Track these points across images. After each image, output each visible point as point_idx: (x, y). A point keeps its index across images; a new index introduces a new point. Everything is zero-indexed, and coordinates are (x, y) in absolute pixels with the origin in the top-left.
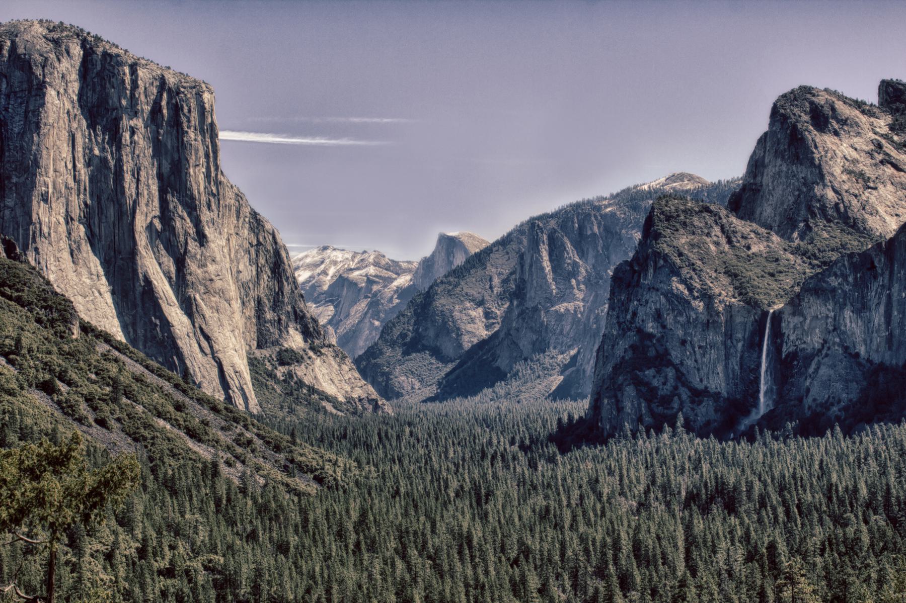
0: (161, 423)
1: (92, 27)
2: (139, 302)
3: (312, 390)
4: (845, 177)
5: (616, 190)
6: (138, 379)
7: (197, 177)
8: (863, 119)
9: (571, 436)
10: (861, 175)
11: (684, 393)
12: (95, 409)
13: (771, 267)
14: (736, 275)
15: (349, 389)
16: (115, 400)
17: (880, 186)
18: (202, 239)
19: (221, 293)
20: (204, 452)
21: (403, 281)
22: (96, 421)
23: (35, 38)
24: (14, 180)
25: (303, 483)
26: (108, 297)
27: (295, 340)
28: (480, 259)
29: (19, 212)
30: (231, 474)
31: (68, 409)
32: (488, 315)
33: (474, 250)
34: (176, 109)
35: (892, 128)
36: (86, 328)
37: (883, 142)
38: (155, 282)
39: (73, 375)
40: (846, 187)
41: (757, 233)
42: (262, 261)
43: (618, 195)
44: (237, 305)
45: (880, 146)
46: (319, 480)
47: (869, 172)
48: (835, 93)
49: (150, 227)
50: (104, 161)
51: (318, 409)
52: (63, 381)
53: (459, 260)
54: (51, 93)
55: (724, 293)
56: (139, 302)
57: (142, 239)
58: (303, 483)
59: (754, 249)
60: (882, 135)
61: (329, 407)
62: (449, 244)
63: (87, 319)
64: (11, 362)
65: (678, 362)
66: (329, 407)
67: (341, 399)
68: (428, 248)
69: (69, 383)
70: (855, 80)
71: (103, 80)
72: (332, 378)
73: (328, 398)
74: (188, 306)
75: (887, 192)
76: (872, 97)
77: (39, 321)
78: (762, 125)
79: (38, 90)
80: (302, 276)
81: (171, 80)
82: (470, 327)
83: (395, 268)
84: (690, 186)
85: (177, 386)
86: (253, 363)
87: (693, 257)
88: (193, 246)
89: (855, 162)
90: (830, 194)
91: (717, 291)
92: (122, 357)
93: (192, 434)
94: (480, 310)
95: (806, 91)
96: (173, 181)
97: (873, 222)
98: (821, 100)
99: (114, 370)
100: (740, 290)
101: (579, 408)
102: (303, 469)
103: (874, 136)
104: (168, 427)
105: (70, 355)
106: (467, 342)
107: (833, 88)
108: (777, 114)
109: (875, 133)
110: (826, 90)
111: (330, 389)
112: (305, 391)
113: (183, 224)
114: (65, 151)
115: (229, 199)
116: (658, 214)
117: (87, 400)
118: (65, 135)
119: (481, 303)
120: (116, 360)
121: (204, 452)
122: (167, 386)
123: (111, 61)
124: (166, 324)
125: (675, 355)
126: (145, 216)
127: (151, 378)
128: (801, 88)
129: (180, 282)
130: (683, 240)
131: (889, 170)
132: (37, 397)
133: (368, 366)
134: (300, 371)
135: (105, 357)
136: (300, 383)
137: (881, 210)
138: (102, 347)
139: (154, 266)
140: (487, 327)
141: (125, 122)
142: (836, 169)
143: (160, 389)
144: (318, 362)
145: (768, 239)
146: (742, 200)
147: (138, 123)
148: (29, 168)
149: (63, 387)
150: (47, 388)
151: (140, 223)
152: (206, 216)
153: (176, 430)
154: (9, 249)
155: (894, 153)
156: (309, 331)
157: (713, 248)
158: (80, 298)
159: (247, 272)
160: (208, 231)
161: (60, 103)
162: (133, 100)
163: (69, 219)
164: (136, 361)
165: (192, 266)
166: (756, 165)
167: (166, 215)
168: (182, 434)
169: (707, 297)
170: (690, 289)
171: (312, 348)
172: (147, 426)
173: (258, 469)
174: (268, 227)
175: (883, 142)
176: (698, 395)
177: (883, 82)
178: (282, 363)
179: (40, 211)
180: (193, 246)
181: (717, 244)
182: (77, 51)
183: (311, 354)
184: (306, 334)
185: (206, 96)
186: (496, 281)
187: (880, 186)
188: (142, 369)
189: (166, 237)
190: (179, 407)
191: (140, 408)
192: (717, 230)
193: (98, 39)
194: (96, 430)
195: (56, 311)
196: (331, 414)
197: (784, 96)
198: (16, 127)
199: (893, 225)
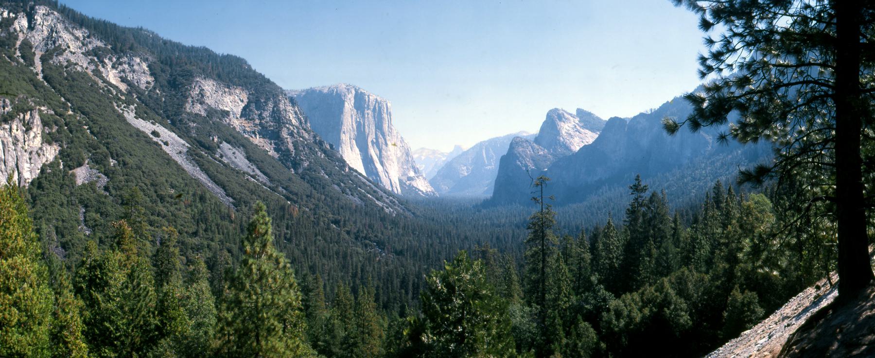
1: (358, 85)
6: (364, 183)
7: (386, 127)
9: (486, 204)
18: (386, 144)
19: (392, 160)
20: (380, 204)
21: (444, 159)
25: (407, 214)
27: (412, 174)
30: (387, 210)
32: (467, 169)
34: (380, 108)
36: (350, 169)
44: (396, 163)
46: (414, 213)
49: (372, 141)
50: (360, 122)
51: (417, 193)
53: (460, 153)
54: (346, 104)
55: (531, 166)
57: (370, 144)
58: (407, 214)
62: (458, 147)
63: (351, 166)
70: (570, 108)
71: (360, 101)
72: (422, 186)
74: (382, 164)
75: (577, 139)
76: (575, 113)
78: (545, 119)
79: (342, 103)
80: (415, 156)
81: (379, 100)
83: (442, 154)
84: (525, 134)
86: (400, 181)
88: (384, 147)
93: (377, 199)
95: (556, 109)
96: (379, 127)
97: (573, 148)
98: (561, 112)
99: (356, 180)
100: (535, 165)
102: (409, 211)
106: (461, 176)
108: (549, 116)
111: (421, 189)
113: (381, 140)
114: (350, 120)
115: (395, 132)
121: (380, 204)
122: (373, 186)
124: (376, 169)
126: (371, 138)
127: (368, 183)
129: (380, 157)
132: (336, 186)
133: (432, 182)
134: (414, 184)
135: (356, 176)
138: (355, 173)
139: (373, 152)
141: (366, 111)
142: (563, 132)
147: (370, 112)
150: (339, 185)
151: (370, 140)
152: (388, 138)
154: (331, 146)
156: (416, 171)
159: (399, 154)
161: (349, 106)
162: (368, 105)
163: (350, 139)
165: (383, 152)
166: (542, 129)
167: (377, 138)
169: (526, 166)
172: (365, 196)
173: (396, 210)
179: (343, 136)
180: (384, 147)
182: (354, 92)
184: (415, 172)
185: (389, 105)
189: (376, 143)
190: (375, 192)
194: (351, 197)
195: (343, 163)
197: (551, 111)
199: (578, 148)
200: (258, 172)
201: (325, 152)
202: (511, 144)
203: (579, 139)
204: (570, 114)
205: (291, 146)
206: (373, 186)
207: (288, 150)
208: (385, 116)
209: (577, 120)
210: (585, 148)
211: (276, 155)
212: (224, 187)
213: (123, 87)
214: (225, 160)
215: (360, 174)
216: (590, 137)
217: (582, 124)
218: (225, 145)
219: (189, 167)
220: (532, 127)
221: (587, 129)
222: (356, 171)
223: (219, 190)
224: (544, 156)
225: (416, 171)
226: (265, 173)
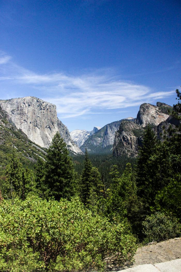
0: (40, 156)
2: (45, 138)
3: (72, 151)
4: (151, 117)
5: (120, 120)
6: (39, 150)
8: (154, 108)
10: (154, 116)
11: (126, 151)
12: (29, 155)
13: (140, 131)
14: (134, 132)
15: (78, 151)
16: (33, 153)
17: (157, 118)
18: (55, 128)
22: (30, 156)
24: (26, 120)
26: (41, 138)
28: (100, 130)
29: (27, 125)
31: (25, 155)
33: (98, 130)
35: (159, 109)
37: (157, 111)
38: (47, 135)
39: (26, 149)
40: (151, 118)
41: (138, 126)
42: (64, 132)
43: (120, 120)
45: (157, 112)
47: (155, 116)
48: (150, 104)
52: (25, 150)
56: (45, 138)
59: (137, 128)
60: (158, 111)
61: (75, 154)
64: (17, 147)
65: (125, 146)
66: (75, 154)
67: (77, 153)
69: (26, 151)
73: (75, 152)
77: (23, 141)
82: (98, 141)
85: (45, 151)
87: (127, 129)
89: (153, 114)
90: (149, 120)
91: (131, 135)
92: (37, 146)
94: (99, 138)
95: (146, 104)
100: (135, 135)
103: (155, 110)
104: (41, 157)
105: (27, 146)
107: (150, 103)
109: (156, 110)
110: (149, 104)
111: (75, 151)
112: (71, 151)
117: (28, 153)
118: (33, 113)
119: (100, 137)
120: (35, 147)
122: (43, 151)
125: (125, 145)
127: (41, 150)
128: (144, 103)
130: (126, 127)
131: (158, 116)
134: (70, 148)
135: (33, 147)
136: (70, 150)
137: (157, 121)
138: (33, 145)
140: (101, 141)
143: (42, 151)
144: (73, 147)
145: (139, 127)
149: (25, 151)
153: (42, 158)
155: (159, 113)
157: (131, 128)
158: (36, 138)
160: (56, 127)
164: (39, 147)
168: (43, 158)
170: (127, 134)
171: (73, 145)
174: (65, 126)
175: (157, 111)
176: (129, 151)
177: (157, 102)
178: (68, 147)
181: (131, 127)
182: (35, 101)
183: (72, 146)
184: (71, 142)
186: (102, 134)
187: (157, 118)
188: (39, 148)
191: (37, 154)
192: (132, 125)
193: (38, 99)
194: (30, 158)
196: (75, 155)
197: (142, 105)
198: (26, 112)
199: (158, 124)
204: (153, 106)
206: (43, 151)
209: (157, 109)
215: (37, 145)
217: (160, 111)
221: (163, 112)
222: (34, 143)
224: (140, 129)
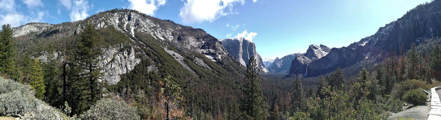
7: (254, 51)
23: (239, 39)
27: (262, 67)
68: (275, 58)
72: (265, 70)
101: (288, 74)
116: (296, 56)
123: (246, 41)
130: (299, 58)
133: (269, 69)
146: (305, 55)
148: (239, 50)
154: (235, 58)
166: (307, 51)
199: (320, 58)
200: (208, 66)
201: (232, 59)
202: (296, 57)
203: (320, 54)
205: (220, 58)
207: (219, 59)
208: (253, 48)
210: (323, 58)
211: (215, 61)
212: (196, 72)
213: (163, 39)
214: (196, 63)
216: (325, 54)
218: (197, 58)
219: (184, 66)
220: (304, 51)
223: (194, 73)
225: (263, 65)
226: (210, 67)
